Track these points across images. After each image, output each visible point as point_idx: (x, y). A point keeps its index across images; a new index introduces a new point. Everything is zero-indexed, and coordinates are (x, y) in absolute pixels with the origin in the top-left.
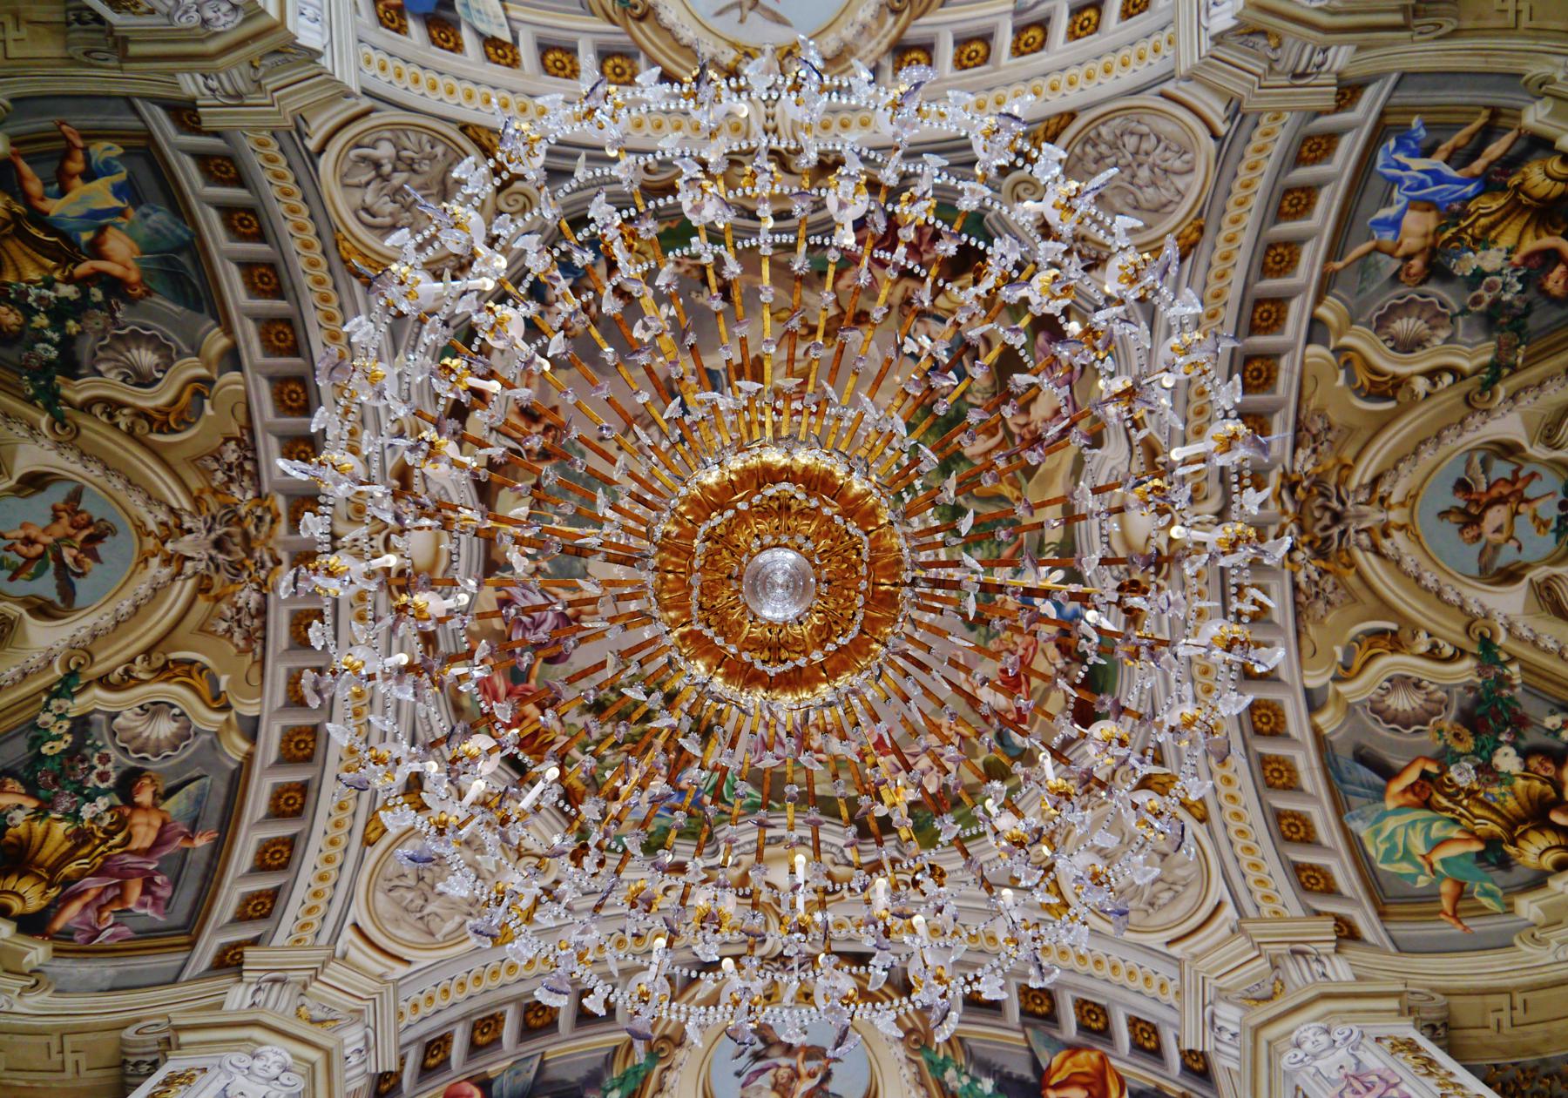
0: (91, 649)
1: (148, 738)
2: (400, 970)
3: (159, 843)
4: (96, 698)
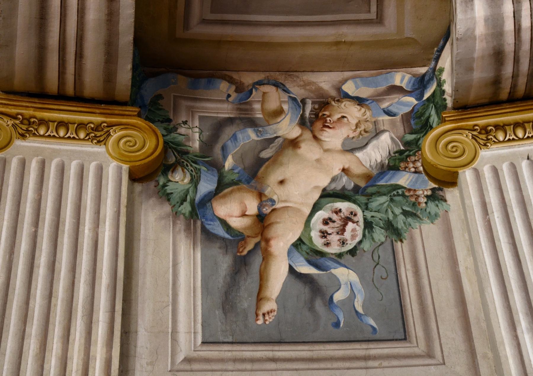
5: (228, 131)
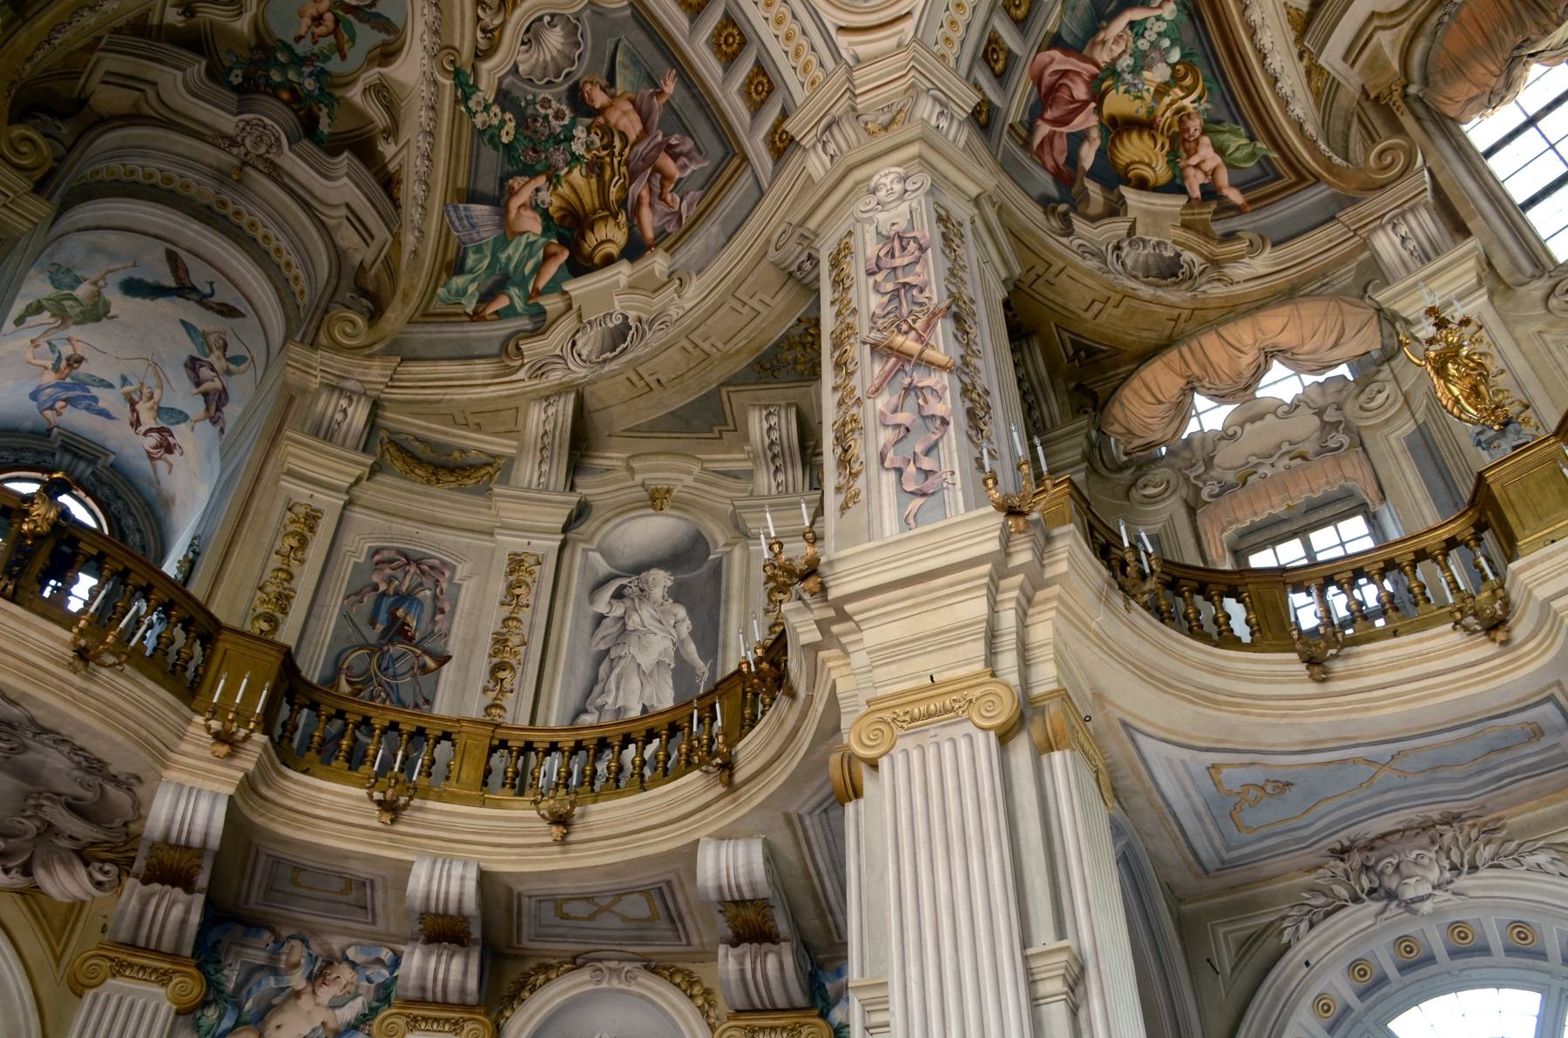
0: (446, 42)
1: (553, 58)
2: (908, 26)
3: (645, 120)
4: (489, 71)
5: (257, 976)
